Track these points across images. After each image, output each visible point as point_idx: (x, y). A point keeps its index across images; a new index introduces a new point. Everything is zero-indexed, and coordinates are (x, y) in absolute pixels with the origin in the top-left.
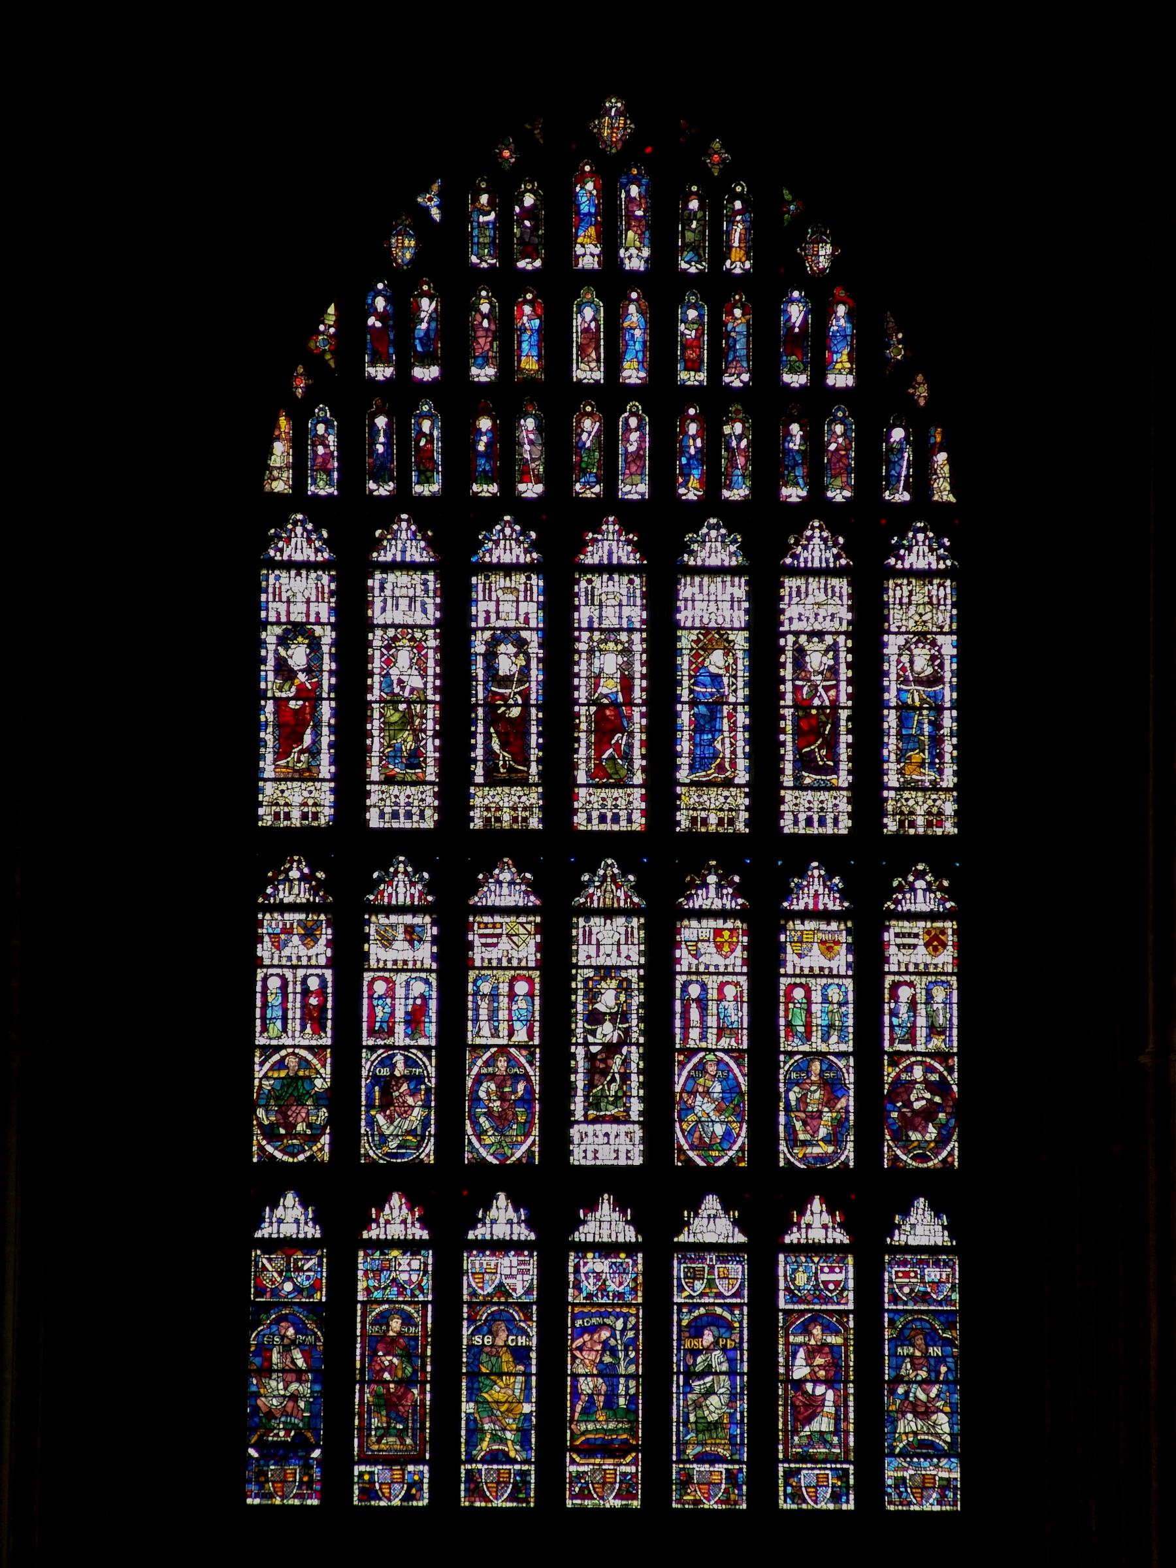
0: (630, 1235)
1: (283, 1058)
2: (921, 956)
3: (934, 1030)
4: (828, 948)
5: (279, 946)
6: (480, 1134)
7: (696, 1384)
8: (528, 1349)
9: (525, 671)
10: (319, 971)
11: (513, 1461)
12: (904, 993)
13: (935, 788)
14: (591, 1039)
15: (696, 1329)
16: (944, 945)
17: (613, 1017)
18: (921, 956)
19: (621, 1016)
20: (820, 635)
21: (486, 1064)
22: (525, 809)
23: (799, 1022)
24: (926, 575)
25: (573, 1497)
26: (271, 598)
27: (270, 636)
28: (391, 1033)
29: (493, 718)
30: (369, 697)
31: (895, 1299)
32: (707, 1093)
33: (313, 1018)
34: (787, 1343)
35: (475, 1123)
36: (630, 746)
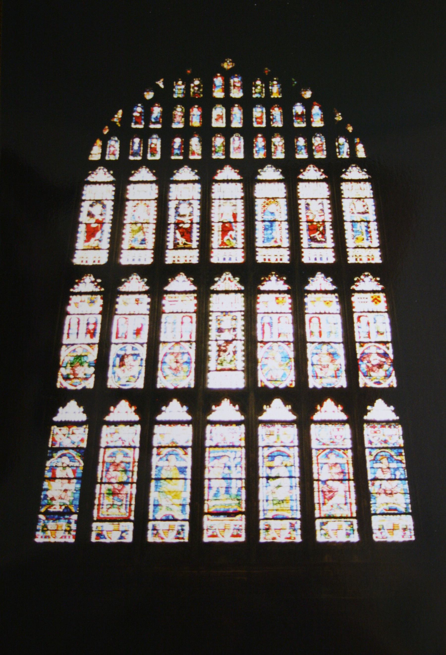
15: (272, 457)
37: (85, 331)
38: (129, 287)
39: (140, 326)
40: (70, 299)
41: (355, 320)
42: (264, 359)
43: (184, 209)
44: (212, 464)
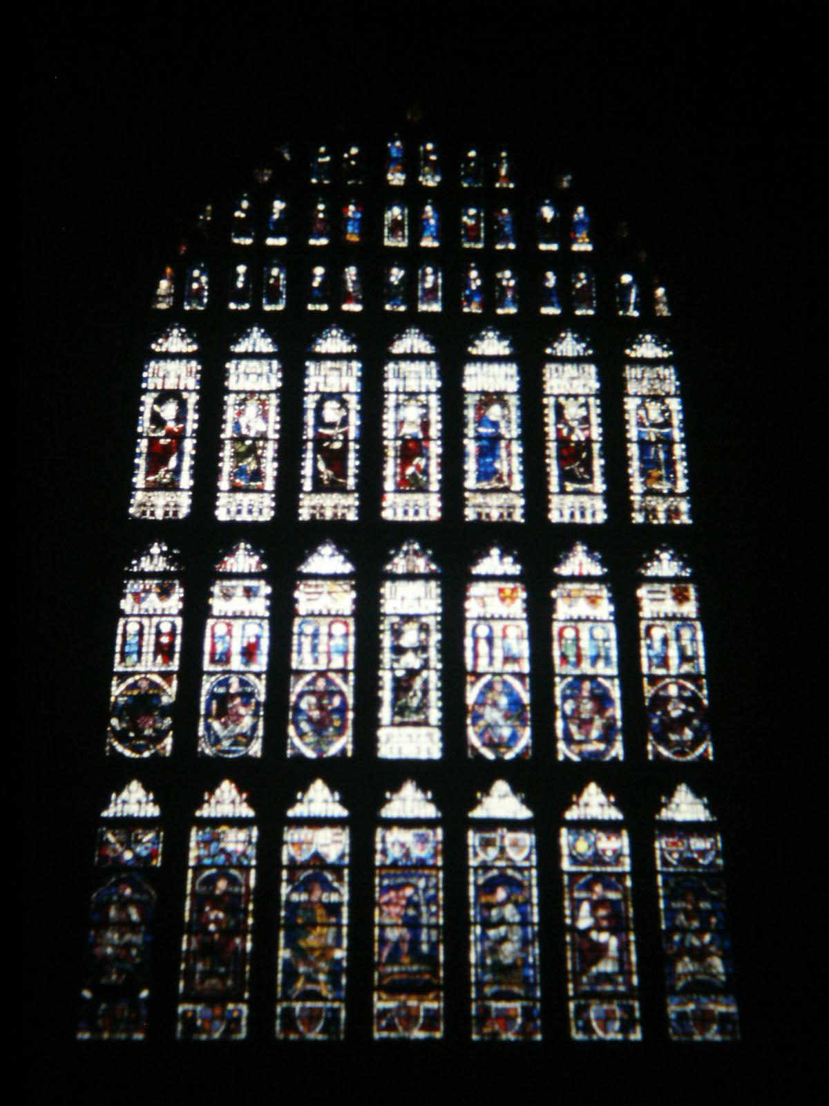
0: (430, 811)
1: (136, 682)
2: (669, 606)
3: (684, 658)
4: (593, 600)
5: (137, 598)
6: (301, 735)
7: (492, 933)
8: (340, 905)
9: (345, 422)
10: (171, 619)
11: (325, 999)
12: (657, 633)
13: (672, 493)
14: (396, 665)
15: (489, 887)
16: (687, 599)
17: (415, 650)
18: (669, 606)
19: (422, 648)
20: (576, 396)
21: (309, 684)
22: (344, 507)
23: (571, 653)
24: (654, 362)
25: (380, 1029)
26: (151, 375)
27: (148, 399)
28: (227, 661)
29: (318, 449)
30: (222, 436)
31: (665, 863)
32: (495, 705)
33: (164, 651)
34: (572, 899)
35: (298, 728)
36: (427, 466)
37: (152, 649)
38: (232, 565)
39: (253, 640)
40: (125, 586)
41: (643, 634)
42: (477, 708)
43: (332, 412)
44: (385, 898)
